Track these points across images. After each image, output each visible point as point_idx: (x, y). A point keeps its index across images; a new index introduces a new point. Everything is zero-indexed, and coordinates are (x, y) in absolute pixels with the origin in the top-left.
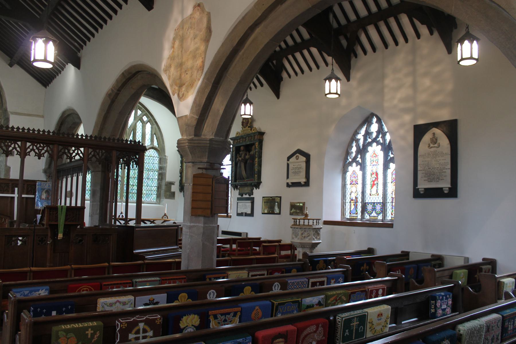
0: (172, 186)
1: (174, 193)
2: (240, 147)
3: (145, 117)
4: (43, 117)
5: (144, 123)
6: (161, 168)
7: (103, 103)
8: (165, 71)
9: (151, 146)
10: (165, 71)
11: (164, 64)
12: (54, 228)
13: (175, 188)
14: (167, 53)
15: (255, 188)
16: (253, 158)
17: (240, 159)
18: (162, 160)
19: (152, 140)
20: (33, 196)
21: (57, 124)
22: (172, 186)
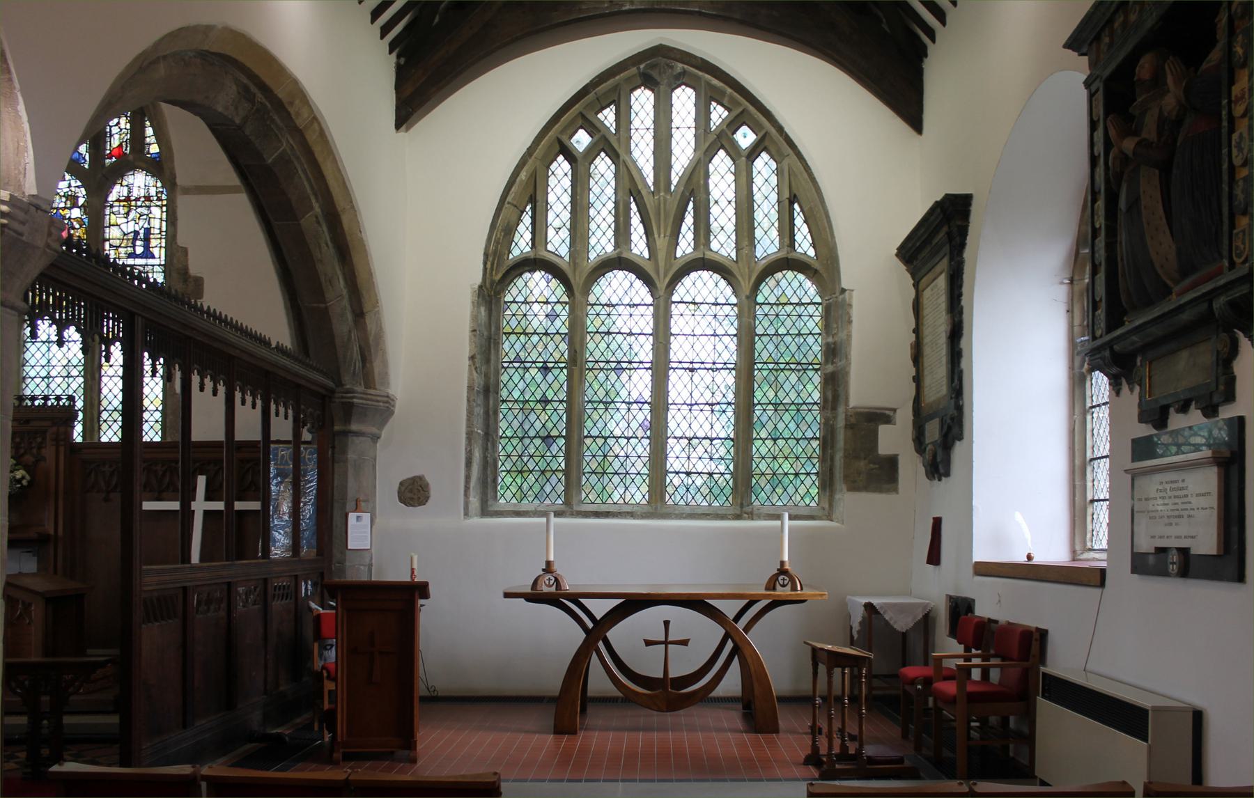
0: (883, 429)
1: (891, 463)
3: (744, 129)
5: (744, 161)
6: (833, 351)
13: (894, 439)
18: (835, 311)
22: (883, 429)
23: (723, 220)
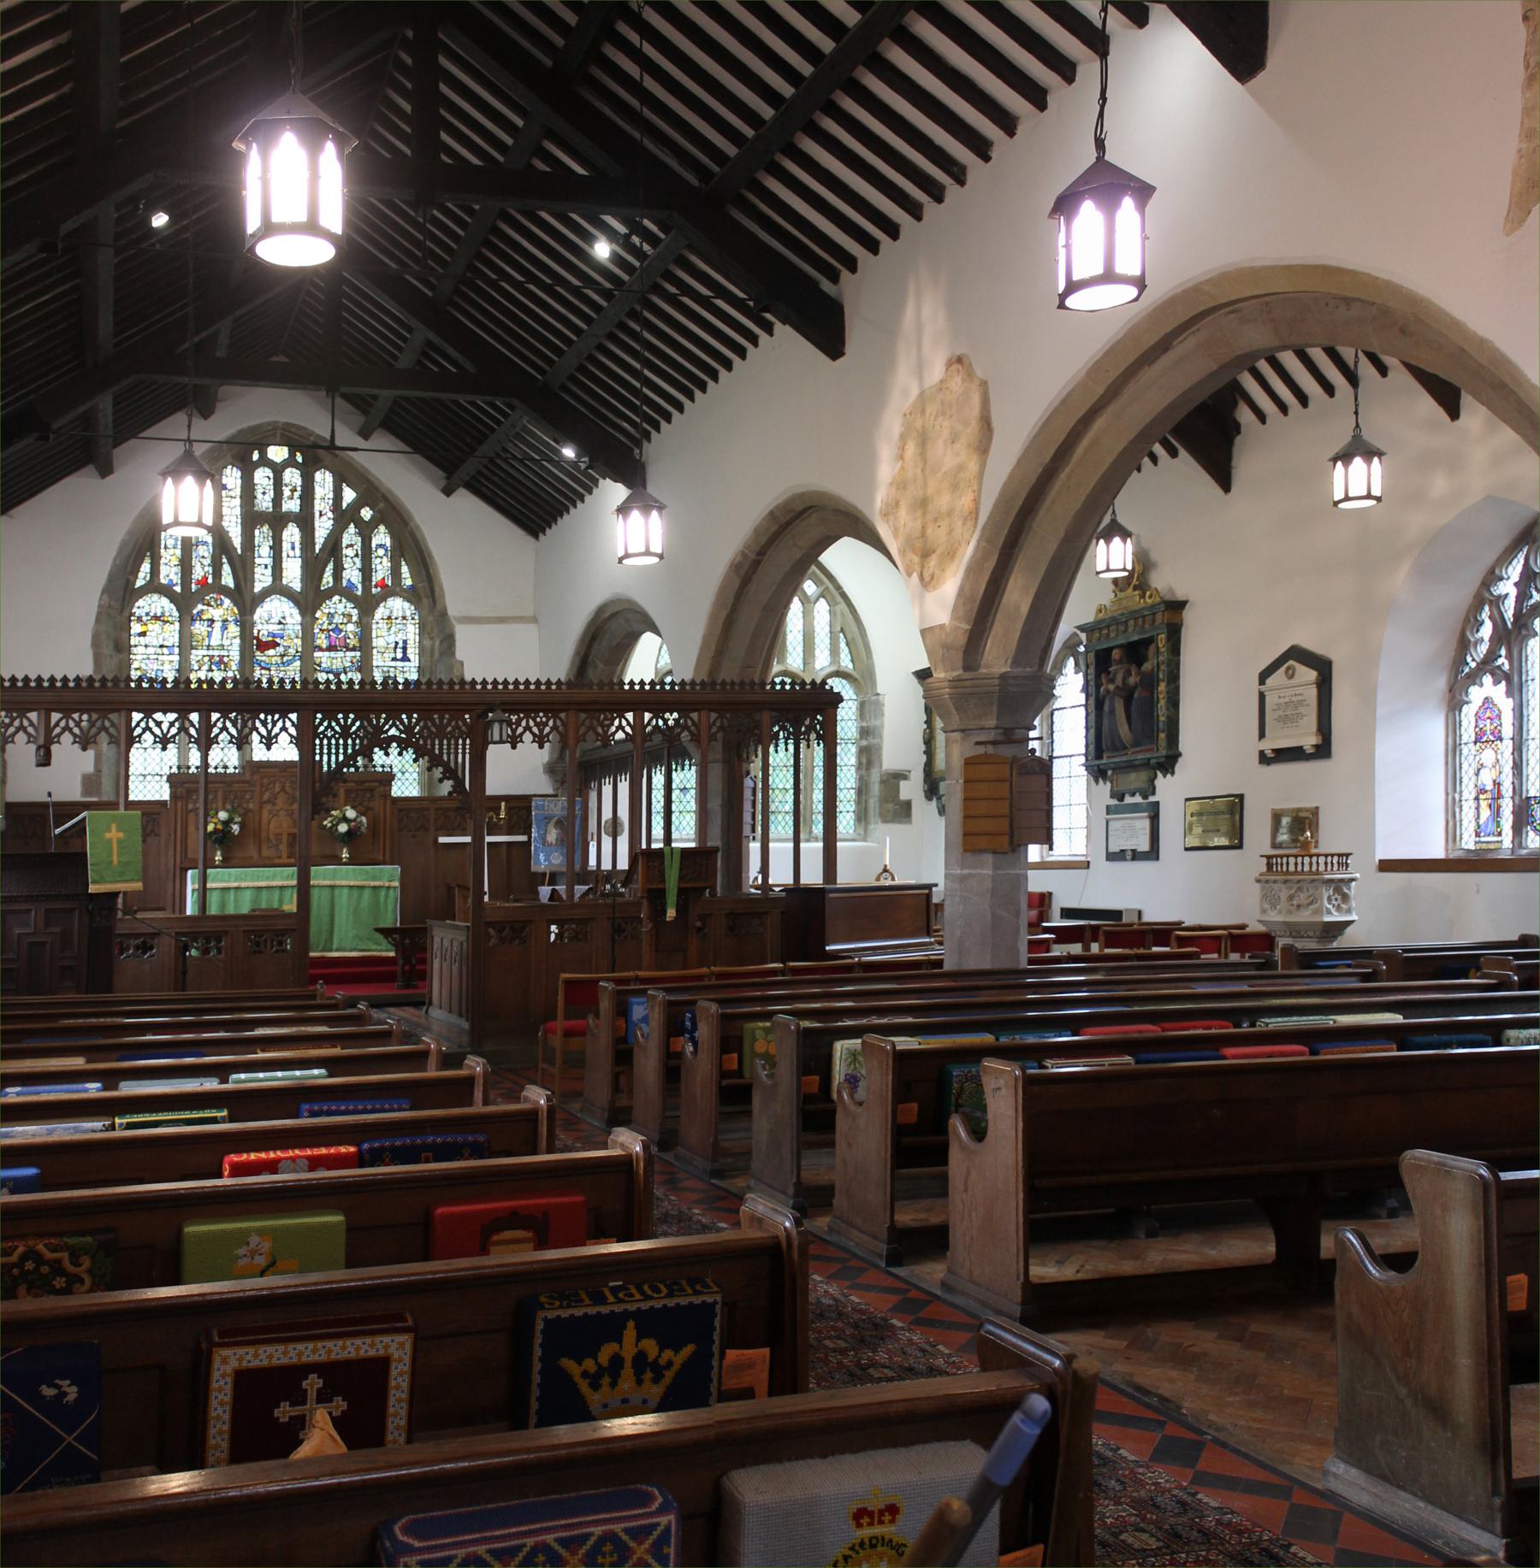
0: (903, 784)
1: (908, 805)
2: (1110, 650)
4: (534, 620)
7: (723, 589)
8: (885, 515)
9: (833, 668)
10: (885, 515)
11: (880, 497)
12: (656, 897)
13: (912, 789)
14: (886, 470)
15: (1159, 775)
16: (1150, 682)
17: (1111, 687)
19: (834, 652)
20: (523, 838)
21: (582, 640)
22: (903, 784)
23: (795, 643)
